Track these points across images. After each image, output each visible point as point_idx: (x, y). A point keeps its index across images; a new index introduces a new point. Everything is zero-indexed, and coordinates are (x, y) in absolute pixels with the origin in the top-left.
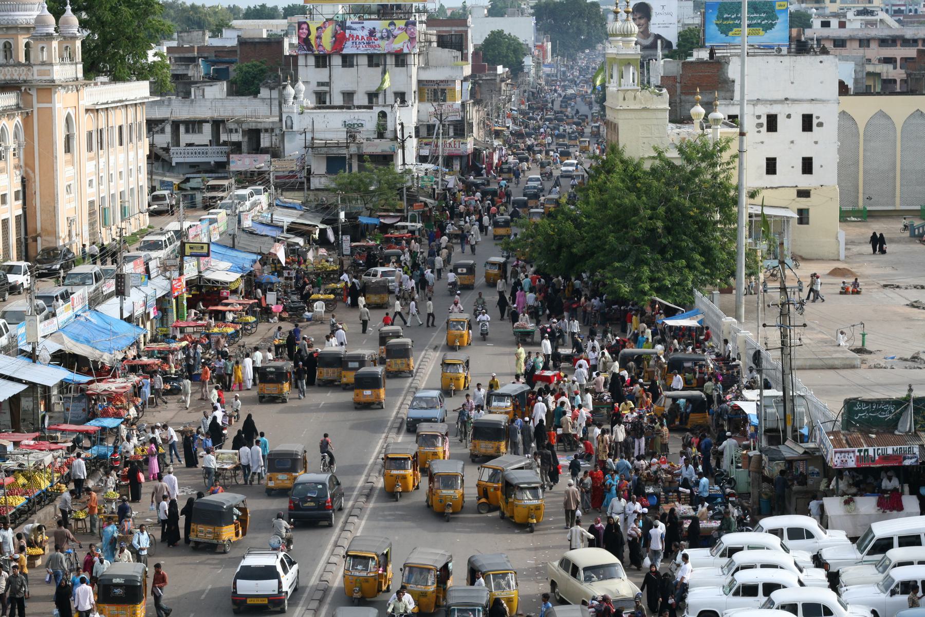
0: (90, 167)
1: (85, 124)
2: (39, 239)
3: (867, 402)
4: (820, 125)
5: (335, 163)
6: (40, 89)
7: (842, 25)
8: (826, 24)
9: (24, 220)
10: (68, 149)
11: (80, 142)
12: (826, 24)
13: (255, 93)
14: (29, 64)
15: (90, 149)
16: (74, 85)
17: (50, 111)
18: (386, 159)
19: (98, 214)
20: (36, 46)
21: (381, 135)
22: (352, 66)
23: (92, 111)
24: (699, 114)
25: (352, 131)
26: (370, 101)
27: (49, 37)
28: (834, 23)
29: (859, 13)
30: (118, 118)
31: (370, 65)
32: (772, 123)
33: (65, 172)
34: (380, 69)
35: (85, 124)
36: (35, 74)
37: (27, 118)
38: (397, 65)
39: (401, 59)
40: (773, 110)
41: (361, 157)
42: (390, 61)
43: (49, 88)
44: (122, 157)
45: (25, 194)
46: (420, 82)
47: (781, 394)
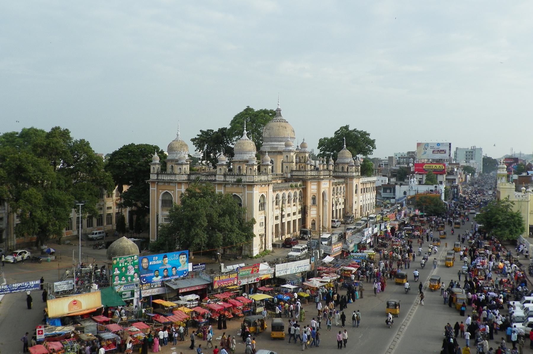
0: (361, 197)
1: (360, 187)
9: (344, 209)
10: (356, 192)
11: (359, 191)
14: (347, 172)
15: (361, 193)
16: (358, 177)
17: (353, 183)
20: (350, 168)
23: (363, 184)
24: (523, 190)
27: (353, 166)
30: (368, 186)
33: (355, 198)
36: (349, 174)
37: (347, 184)
43: (352, 178)
44: (369, 195)
45: (345, 203)
46: (446, 179)
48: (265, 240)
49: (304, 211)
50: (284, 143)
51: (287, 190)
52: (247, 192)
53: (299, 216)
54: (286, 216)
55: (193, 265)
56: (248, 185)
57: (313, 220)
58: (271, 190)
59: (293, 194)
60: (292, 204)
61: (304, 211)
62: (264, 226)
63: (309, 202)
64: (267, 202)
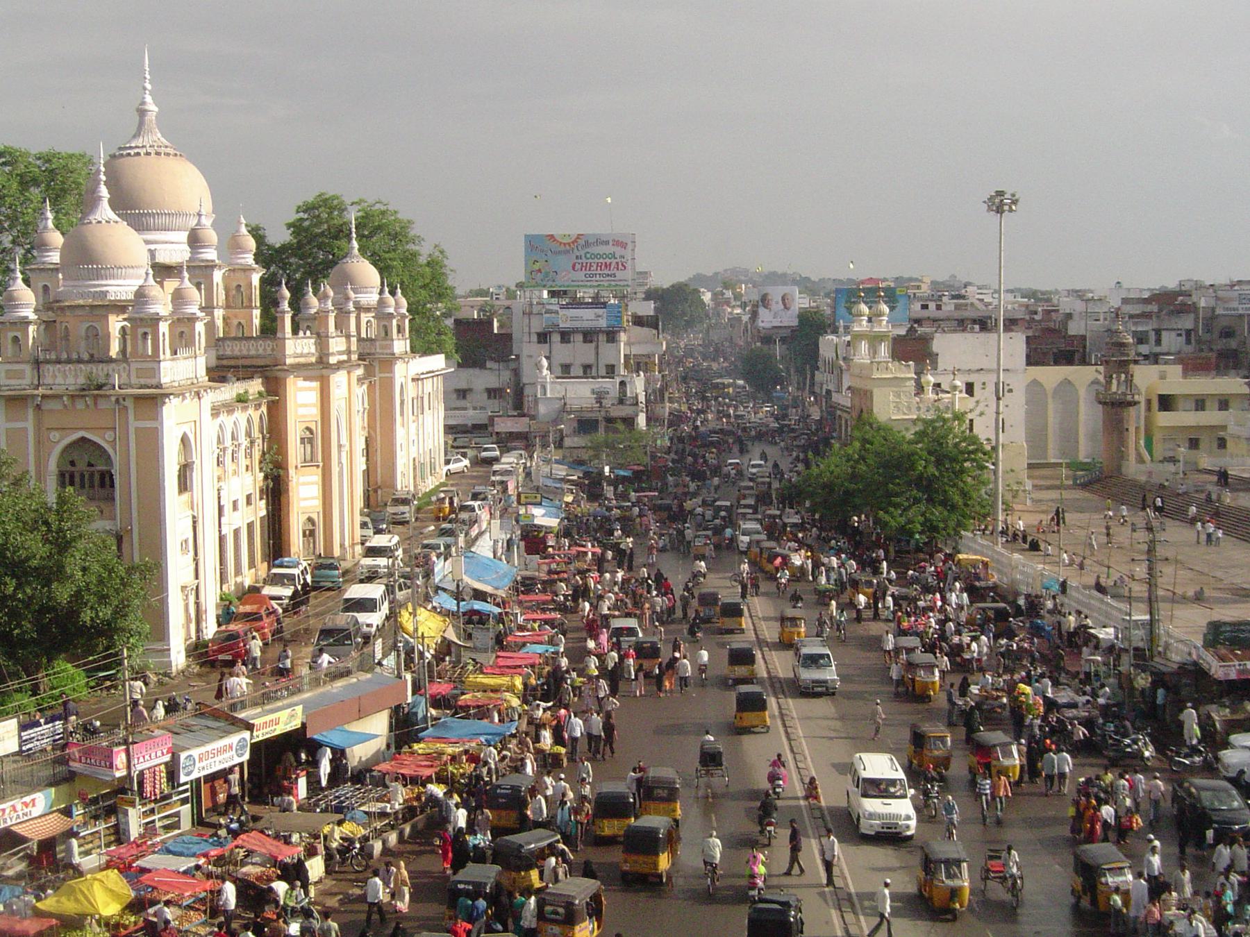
1: (411, 391)
2: (379, 492)
3: (1230, 624)
4: (1010, 391)
5: (586, 425)
6: (382, 361)
7: (939, 307)
8: (925, 307)
10: (402, 414)
12: (925, 307)
13: (482, 366)
18: (630, 422)
19: (419, 469)
21: (621, 401)
22: (569, 342)
25: (600, 396)
26: (585, 372)
28: (932, 306)
29: (954, 297)
31: (585, 341)
32: (970, 389)
33: (400, 433)
34: (593, 345)
35: (411, 391)
38: (608, 341)
39: (612, 336)
40: (970, 379)
41: (610, 420)
42: (602, 338)
47: (1148, 617)
48: (197, 604)
49: (275, 492)
50: (183, 236)
51: (230, 411)
52: (133, 424)
53: (261, 508)
54: (228, 508)
55: (23, 727)
56: (138, 398)
57: (310, 520)
58: (207, 412)
59: (243, 425)
60: (244, 462)
61: (275, 492)
62: (192, 553)
63: (295, 452)
64: (197, 462)
